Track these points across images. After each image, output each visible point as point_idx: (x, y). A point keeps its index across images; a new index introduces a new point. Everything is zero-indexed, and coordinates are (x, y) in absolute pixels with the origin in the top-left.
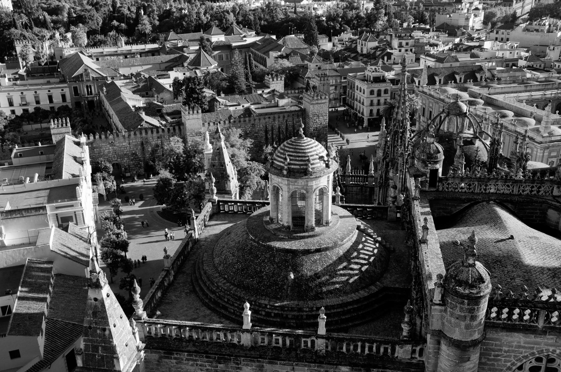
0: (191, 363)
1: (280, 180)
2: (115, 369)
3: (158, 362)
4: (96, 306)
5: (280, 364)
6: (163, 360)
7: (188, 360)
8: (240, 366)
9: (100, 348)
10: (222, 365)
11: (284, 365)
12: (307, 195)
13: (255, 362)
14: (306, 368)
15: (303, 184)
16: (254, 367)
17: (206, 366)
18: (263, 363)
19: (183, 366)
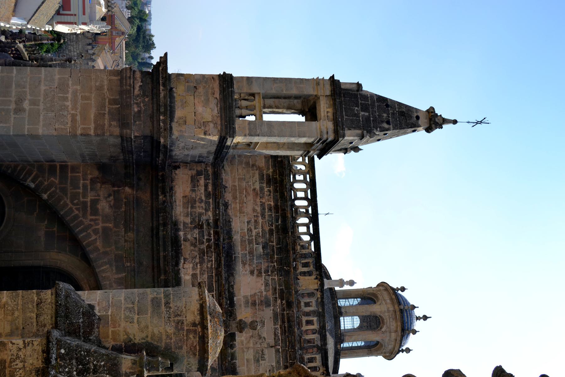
0: (259, 209)
1: (388, 301)
2: (346, 129)
3: (253, 165)
4: (411, 117)
5: (276, 329)
6: (257, 172)
7: (262, 205)
8: (263, 274)
9: (367, 114)
10: (261, 250)
11: (275, 334)
12: (379, 332)
13: (273, 294)
14: (274, 364)
15: (392, 327)
16: (264, 293)
17: (255, 228)
18: (274, 306)
19: (251, 197)
